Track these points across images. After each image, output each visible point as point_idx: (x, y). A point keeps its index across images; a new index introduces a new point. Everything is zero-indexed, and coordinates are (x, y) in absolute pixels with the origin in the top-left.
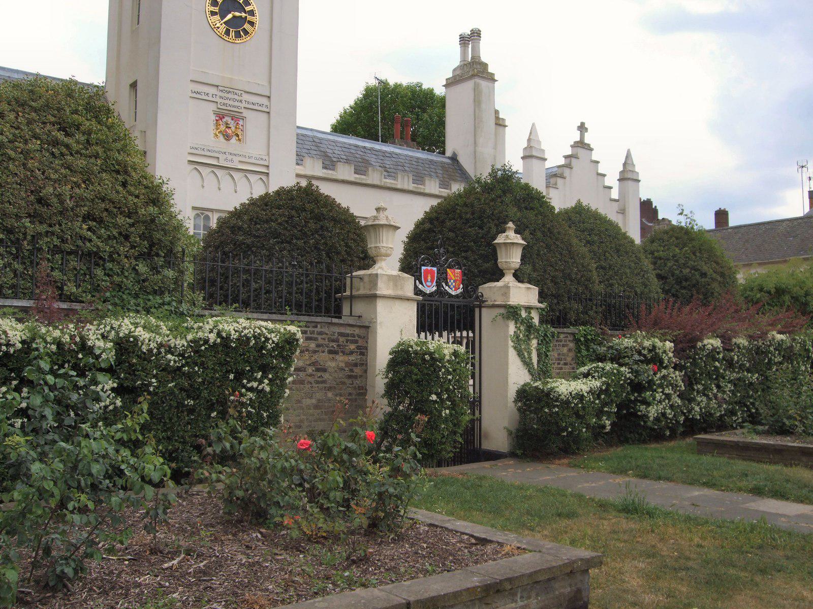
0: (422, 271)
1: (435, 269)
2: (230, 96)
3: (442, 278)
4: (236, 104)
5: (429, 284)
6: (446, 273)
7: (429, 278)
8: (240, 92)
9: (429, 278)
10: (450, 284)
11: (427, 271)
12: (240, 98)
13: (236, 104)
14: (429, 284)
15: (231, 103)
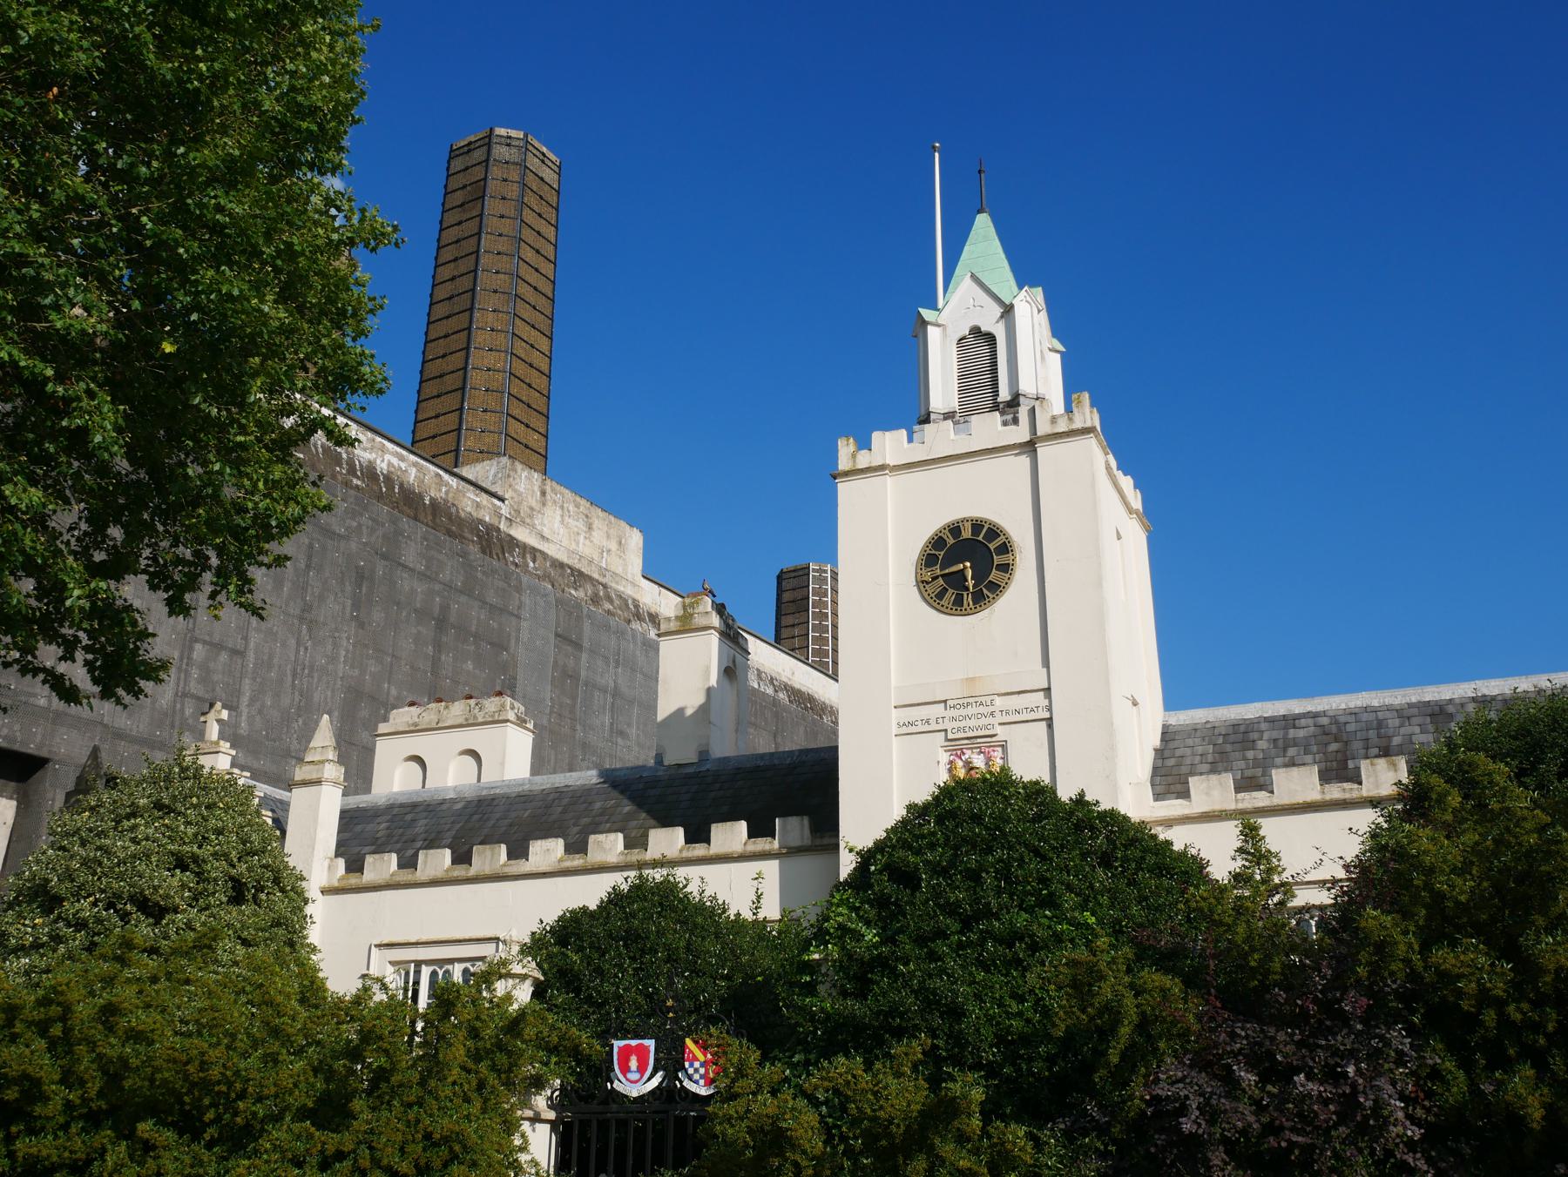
0: (616, 1050)
1: (650, 1044)
2: (970, 711)
3: (671, 1061)
4: (984, 721)
5: (634, 1076)
6: (683, 1045)
7: (633, 1064)
8: (988, 699)
9: (633, 1064)
10: (691, 1071)
11: (626, 1053)
12: (991, 709)
13: (984, 721)
14: (634, 1076)
15: (972, 723)
